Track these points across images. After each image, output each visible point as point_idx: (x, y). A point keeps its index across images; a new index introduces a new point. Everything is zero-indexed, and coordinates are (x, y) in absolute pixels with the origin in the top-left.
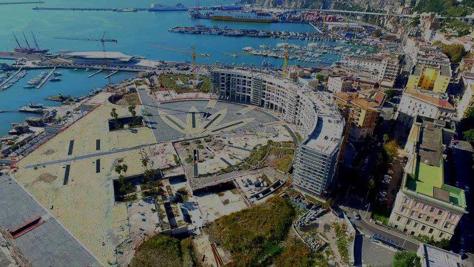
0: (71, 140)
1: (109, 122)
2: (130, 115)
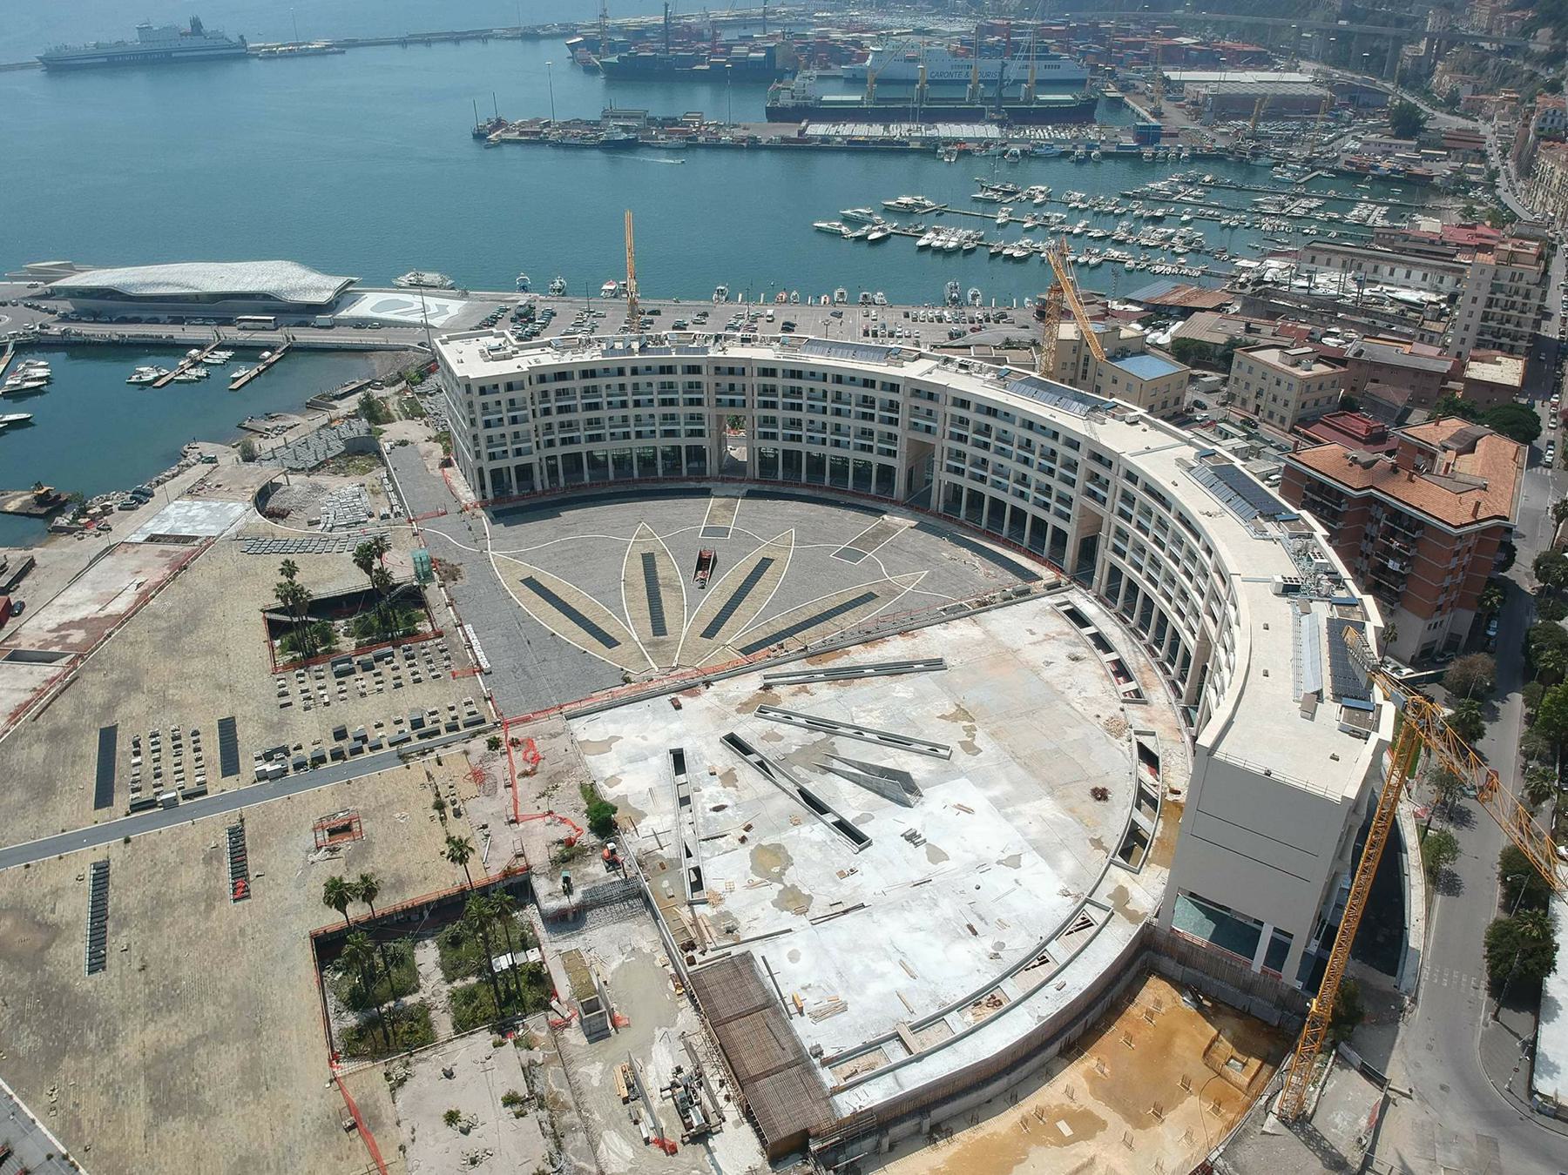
0: (105, 725)
1: (271, 623)
2: (359, 581)
